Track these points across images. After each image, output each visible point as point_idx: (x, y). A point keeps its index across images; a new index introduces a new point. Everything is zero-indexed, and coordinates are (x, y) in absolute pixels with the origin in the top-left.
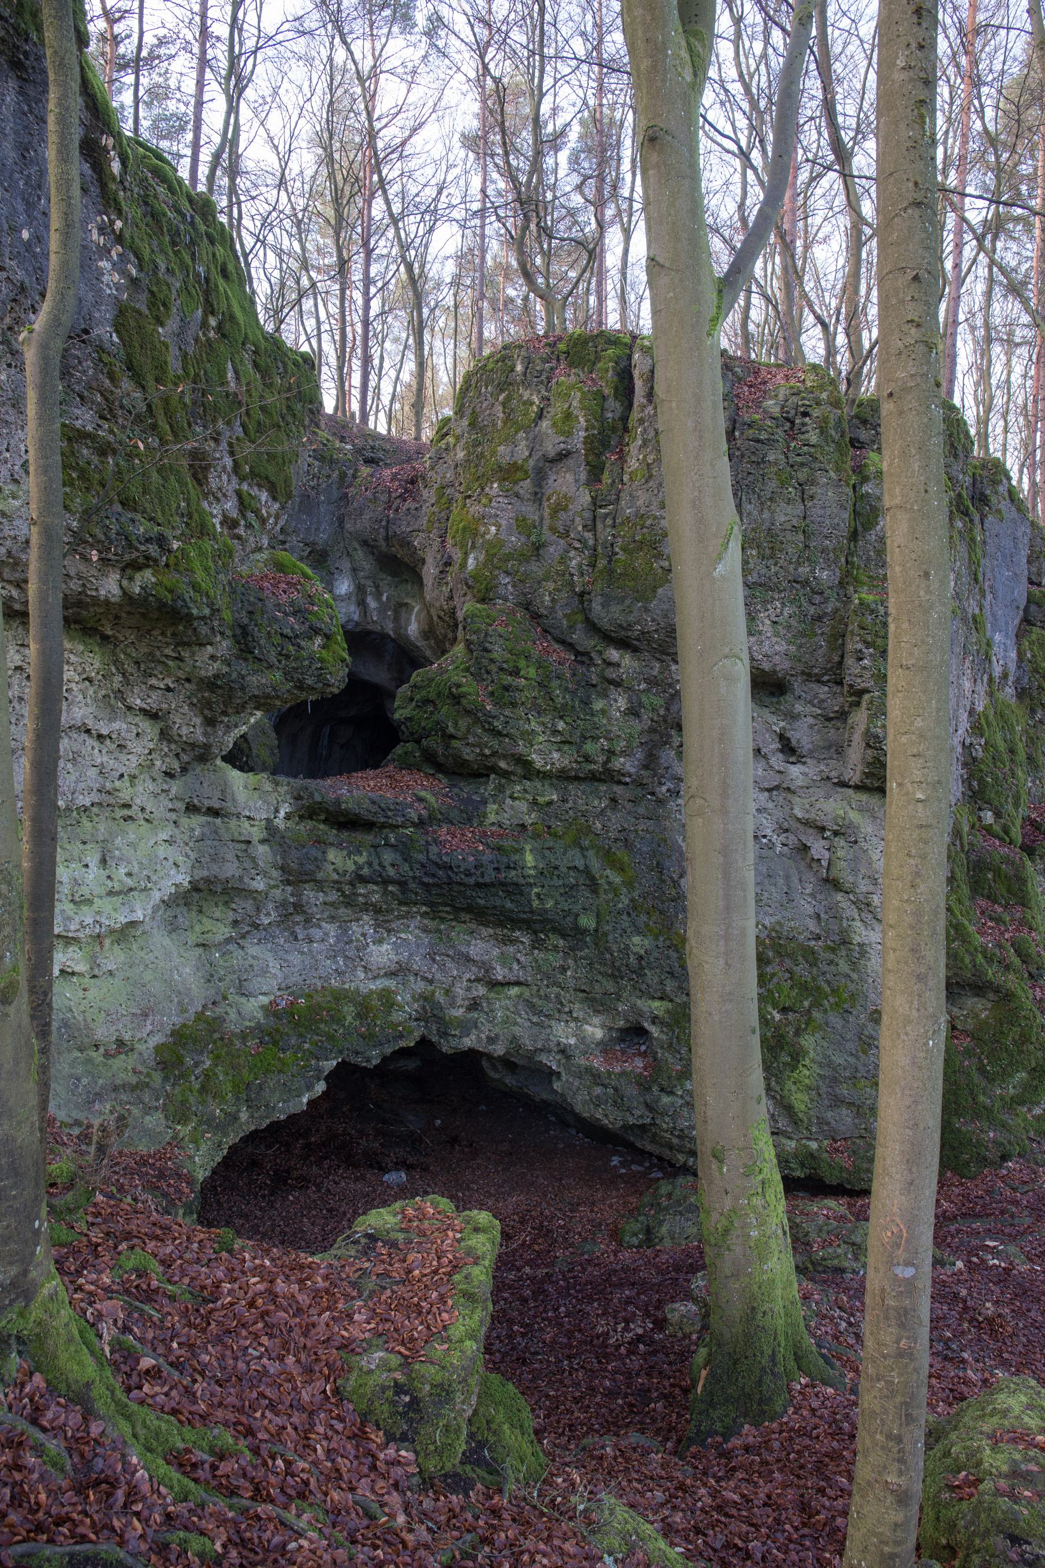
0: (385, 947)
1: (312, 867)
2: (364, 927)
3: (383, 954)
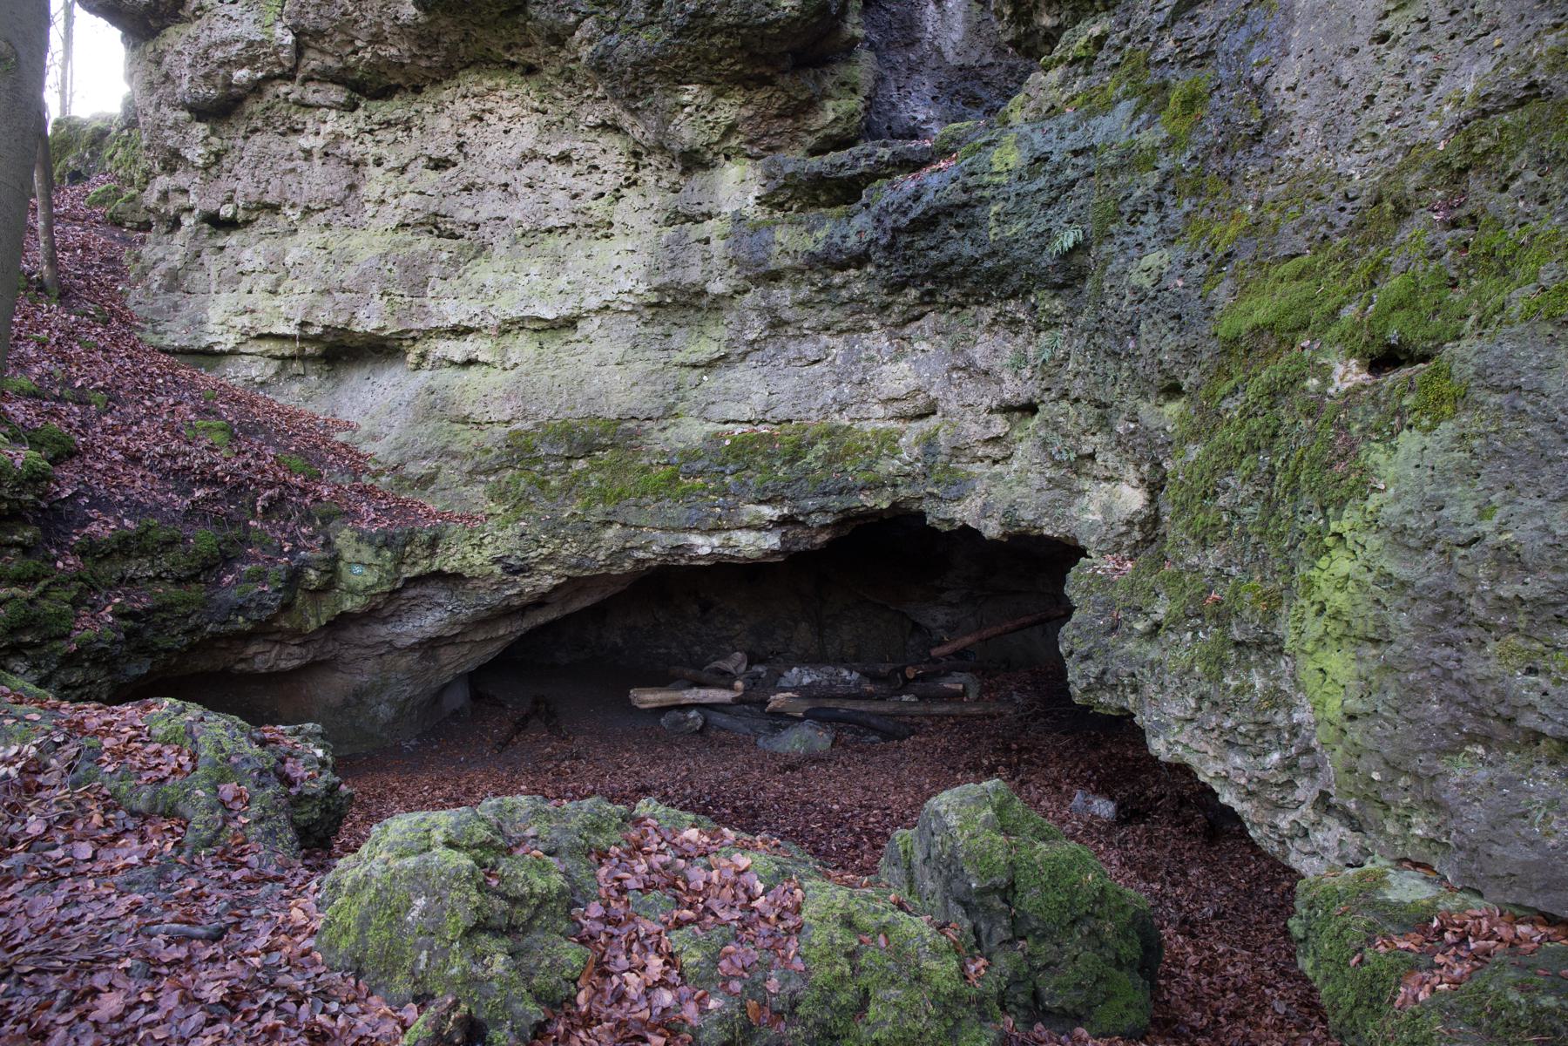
0: (903, 365)
1: (763, 255)
2: (877, 341)
3: (898, 377)
